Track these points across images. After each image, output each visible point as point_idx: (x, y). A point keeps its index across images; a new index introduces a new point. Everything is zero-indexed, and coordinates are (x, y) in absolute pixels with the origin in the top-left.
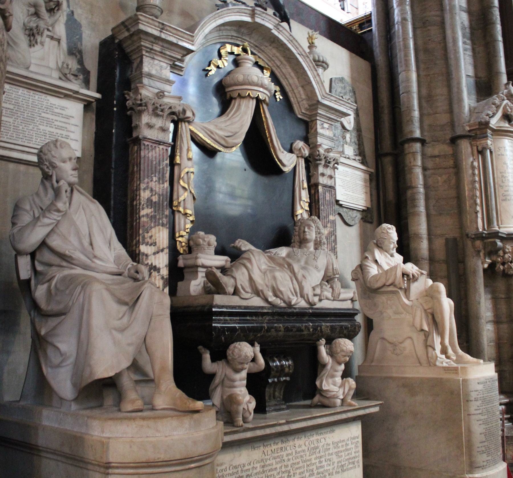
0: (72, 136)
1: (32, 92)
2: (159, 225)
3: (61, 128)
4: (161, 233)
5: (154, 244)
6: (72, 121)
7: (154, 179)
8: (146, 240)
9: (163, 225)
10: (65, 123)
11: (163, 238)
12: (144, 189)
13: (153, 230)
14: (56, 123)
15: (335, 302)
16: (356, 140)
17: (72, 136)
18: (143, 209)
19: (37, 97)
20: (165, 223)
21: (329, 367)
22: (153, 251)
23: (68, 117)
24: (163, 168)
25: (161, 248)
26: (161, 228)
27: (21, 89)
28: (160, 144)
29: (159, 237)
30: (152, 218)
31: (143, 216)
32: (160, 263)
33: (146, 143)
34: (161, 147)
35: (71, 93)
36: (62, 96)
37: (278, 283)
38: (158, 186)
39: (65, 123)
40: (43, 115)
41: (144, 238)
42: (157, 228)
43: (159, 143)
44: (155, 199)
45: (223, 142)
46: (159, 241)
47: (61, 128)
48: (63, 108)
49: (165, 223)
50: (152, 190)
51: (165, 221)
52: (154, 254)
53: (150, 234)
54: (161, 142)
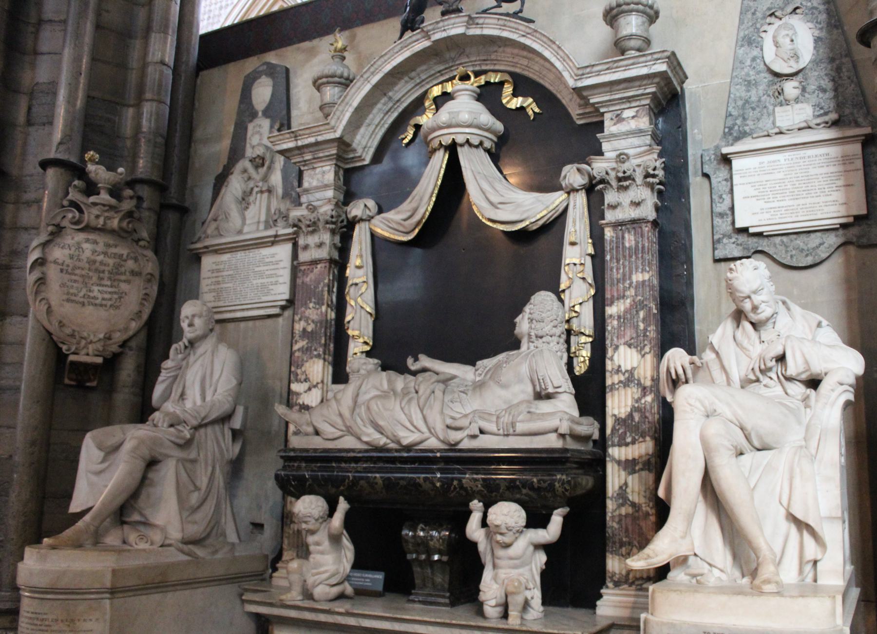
0: (281, 280)
1: (247, 251)
2: (312, 358)
3: (271, 276)
4: (316, 367)
5: (306, 380)
6: (282, 265)
7: (311, 305)
8: (299, 377)
9: (318, 356)
10: (274, 269)
11: (318, 372)
12: (300, 320)
13: (307, 365)
14: (267, 273)
15: (510, 438)
16: (827, 84)
17: (281, 280)
18: (296, 342)
19: (251, 254)
20: (321, 353)
21: (482, 547)
22: (306, 388)
23: (277, 263)
24: (322, 291)
25: (315, 383)
26: (316, 360)
27: (239, 253)
28: (317, 264)
29: (313, 371)
30: (306, 350)
31: (295, 351)
32: (312, 402)
33: (302, 268)
34: (319, 266)
35: (272, 239)
36: (270, 244)
37: (373, 413)
38: (315, 312)
39: (274, 269)
40: (257, 269)
41: (297, 375)
42: (311, 361)
43: (314, 262)
44: (309, 329)
45: (401, 229)
46: (313, 375)
47: (271, 276)
48: (273, 256)
49: (321, 353)
50: (307, 319)
51: (321, 350)
52: (305, 392)
53: (303, 369)
54: (316, 261)
